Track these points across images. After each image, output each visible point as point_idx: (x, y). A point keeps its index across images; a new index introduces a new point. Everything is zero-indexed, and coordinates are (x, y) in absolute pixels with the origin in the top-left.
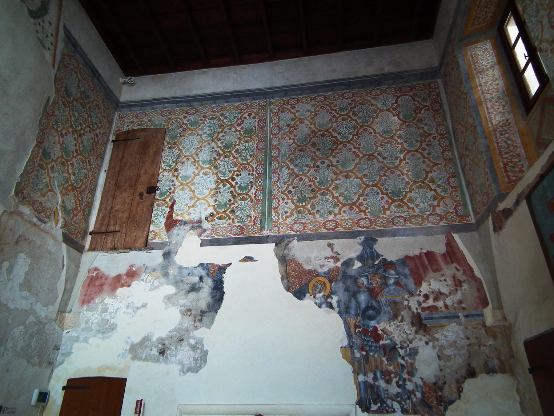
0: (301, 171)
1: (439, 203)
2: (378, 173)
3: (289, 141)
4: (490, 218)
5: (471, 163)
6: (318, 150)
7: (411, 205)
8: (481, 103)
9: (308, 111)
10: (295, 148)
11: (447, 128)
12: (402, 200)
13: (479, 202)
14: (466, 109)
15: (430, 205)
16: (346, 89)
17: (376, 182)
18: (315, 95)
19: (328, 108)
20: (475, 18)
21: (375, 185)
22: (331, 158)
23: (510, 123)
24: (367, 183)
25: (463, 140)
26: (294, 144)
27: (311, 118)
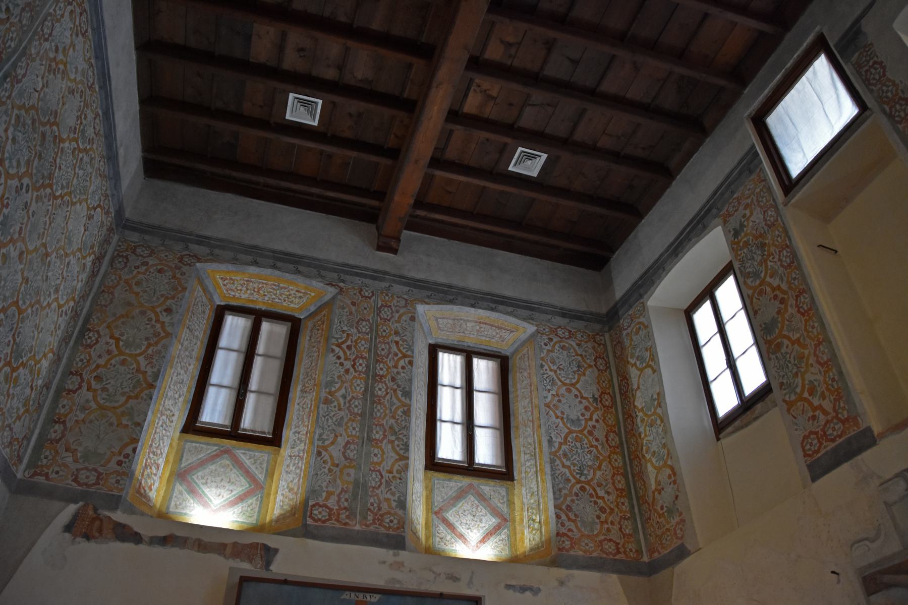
0: (10, 161)
1: (23, 414)
2: (33, 293)
3: (40, 79)
4: (72, 508)
5: (93, 405)
6: (40, 157)
7: (11, 391)
8: (171, 367)
9: (76, 68)
10: (33, 107)
11: (82, 310)
12: (14, 370)
13: (66, 466)
14: (149, 345)
15: (18, 409)
16: (103, 113)
17: (24, 307)
18: (93, 61)
19: (82, 104)
20: (231, 279)
21: (20, 312)
22: (35, 194)
23: (172, 422)
24: (21, 296)
25: (102, 362)
26: (37, 94)
27: (69, 88)
